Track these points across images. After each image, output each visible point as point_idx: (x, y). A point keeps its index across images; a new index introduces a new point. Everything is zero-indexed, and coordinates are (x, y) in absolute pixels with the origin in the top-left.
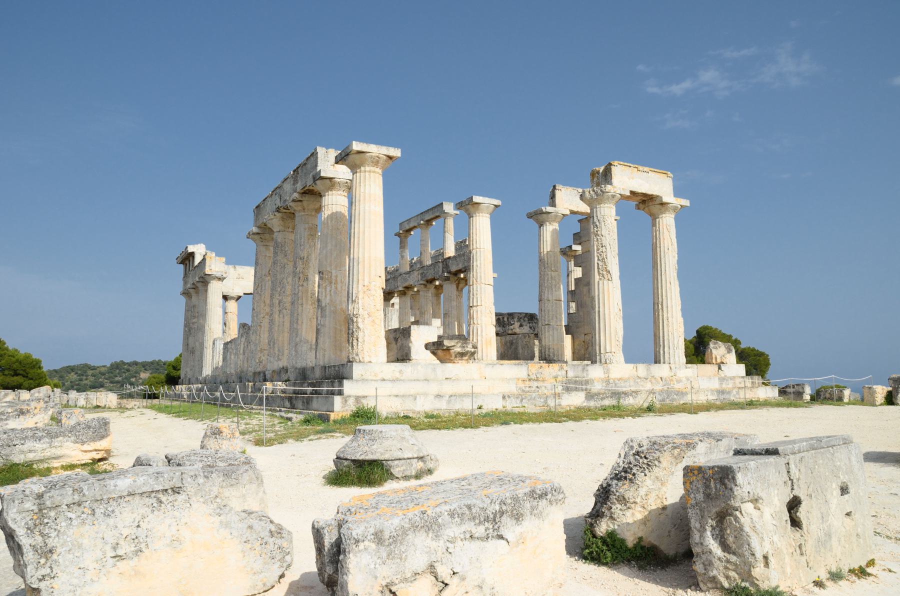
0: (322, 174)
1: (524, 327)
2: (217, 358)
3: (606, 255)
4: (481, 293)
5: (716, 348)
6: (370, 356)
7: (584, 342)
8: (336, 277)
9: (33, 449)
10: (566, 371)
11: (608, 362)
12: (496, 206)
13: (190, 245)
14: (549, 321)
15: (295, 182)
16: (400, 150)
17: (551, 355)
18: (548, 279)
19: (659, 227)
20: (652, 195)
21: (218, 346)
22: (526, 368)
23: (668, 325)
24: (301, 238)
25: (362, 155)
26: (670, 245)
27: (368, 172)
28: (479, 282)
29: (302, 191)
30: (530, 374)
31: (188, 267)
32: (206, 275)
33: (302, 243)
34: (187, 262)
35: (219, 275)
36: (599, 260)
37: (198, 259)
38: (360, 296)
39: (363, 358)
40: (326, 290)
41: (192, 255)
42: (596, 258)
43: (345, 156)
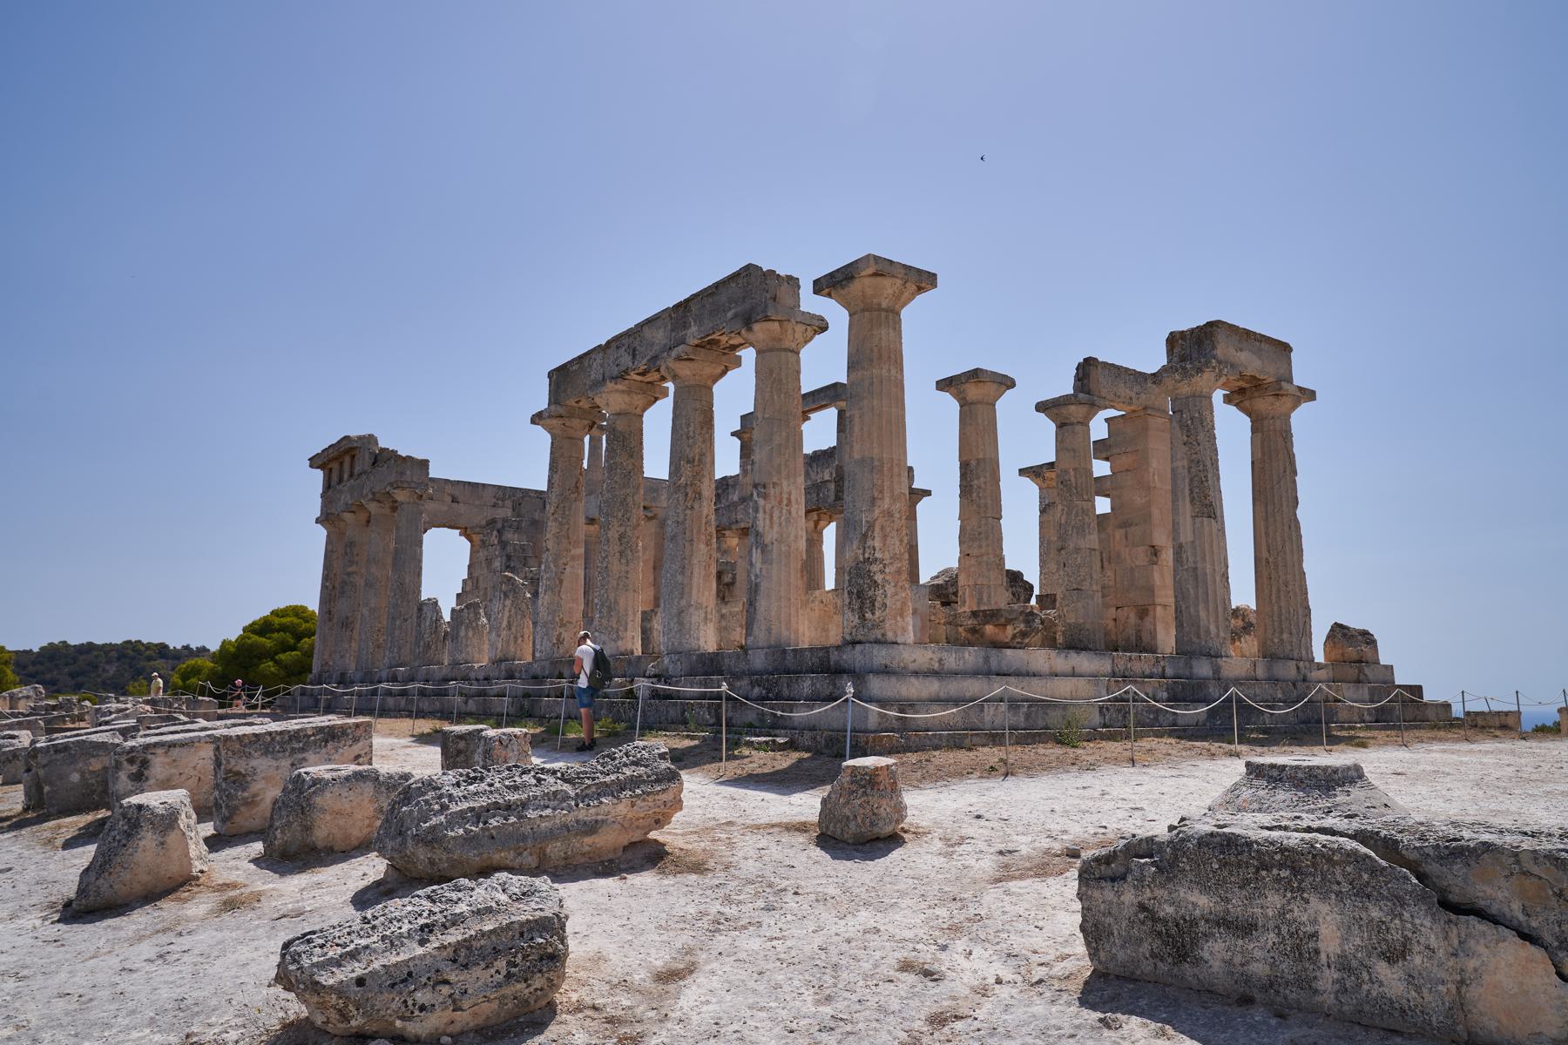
3: (1206, 477)
7: (1115, 620)
18: (1077, 513)
22: (1110, 661)
24: (688, 426)
29: (696, 342)
33: (691, 434)
40: (771, 517)
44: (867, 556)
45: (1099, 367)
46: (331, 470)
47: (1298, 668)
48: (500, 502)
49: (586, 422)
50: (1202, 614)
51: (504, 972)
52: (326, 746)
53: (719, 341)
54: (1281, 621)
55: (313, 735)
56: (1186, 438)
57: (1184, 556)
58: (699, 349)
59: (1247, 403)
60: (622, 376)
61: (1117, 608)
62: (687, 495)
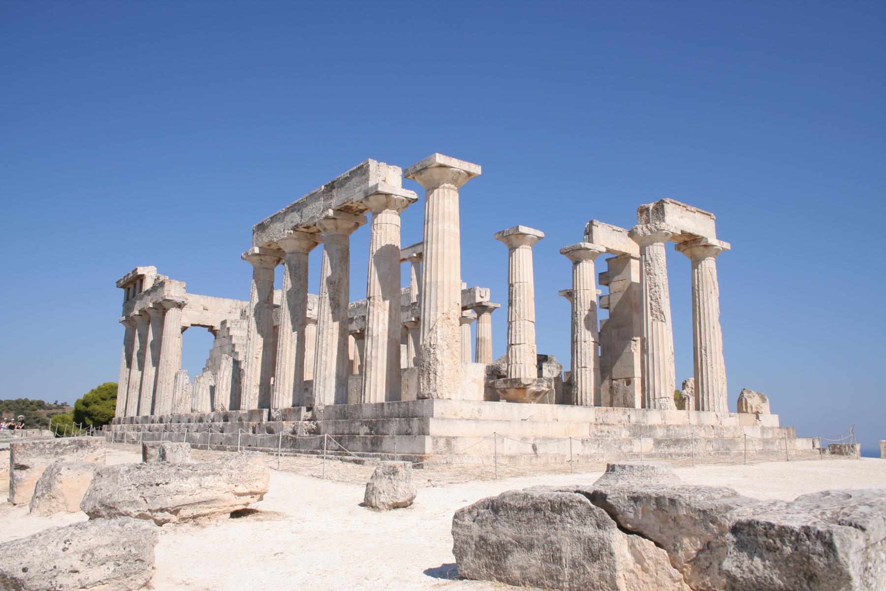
0: (380, 189)
2: (180, 394)
4: (524, 331)
5: (750, 397)
6: (449, 393)
9: (180, 489)
10: (629, 416)
11: (663, 407)
12: (539, 238)
13: (140, 266)
14: (586, 363)
16: (480, 167)
17: (588, 399)
19: (701, 269)
20: (698, 236)
21: (181, 381)
23: (711, 371)
26: (713, 288)
27: (447, 188)
28: (522, 319)
30: (597, 418)
32: (166, 300)
35: (179, 300)
36: (652, 299)
37: (148, 285)
38: (439, 324)
39: (442, 394)
41: (141, 278)
42: (649, 299)
46: (129, 289)
48: (234, 310)
52: (77, 451)
53: (352, 207)
55: (69, 444)
59: (688, 251)
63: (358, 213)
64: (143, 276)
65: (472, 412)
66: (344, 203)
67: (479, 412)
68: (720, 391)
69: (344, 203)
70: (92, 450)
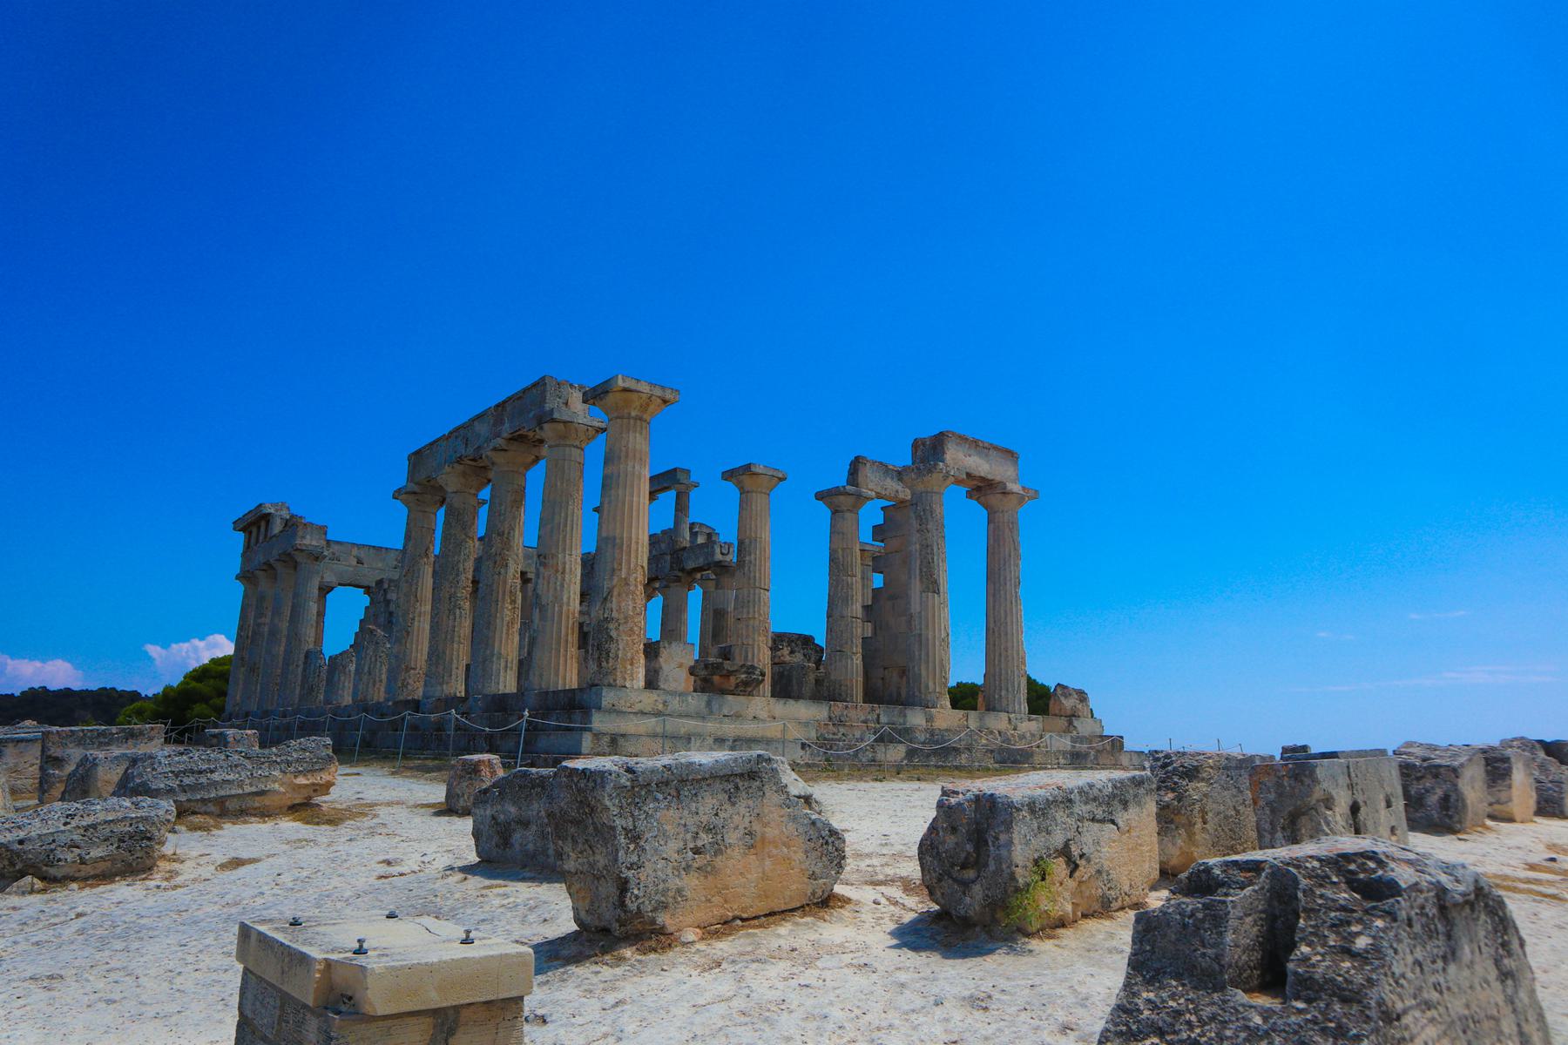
0: (556, 415)
1: (796, 654)
5: (1066, 697)
7: (883, 679)
8: (565, 563)
14: (841, 646)
15: (499, 421)
18: (843, 586)
22: (828, 708)
25: (628, 394)
29: (510, 436)
31: (254, 534)
32: (297, 549)
33: (503, 512)
34: (254, 530)
40: (549, 583)
43: (602, 393)
44: (606, 616)
45: (868, 465)
46: (250, 533)
47: (1010, 720)
49: (438, 498)
50: (924, 673)
51: (116, 845)
52: (126, 742)
54: (1001, 680)
56: (919, 527)
57: (913, 623)
58: (511, 442)
59: (982, 499)
60: (460, 460)
61: (885, 669)
62: (495, 562)
63: (536, 444)
64: (269, 514)
65: (655, 705)
66: (517, 431)
67: (664, 705)
68: (1016, 686)
69: (517, 431)
70: (146, 740)
